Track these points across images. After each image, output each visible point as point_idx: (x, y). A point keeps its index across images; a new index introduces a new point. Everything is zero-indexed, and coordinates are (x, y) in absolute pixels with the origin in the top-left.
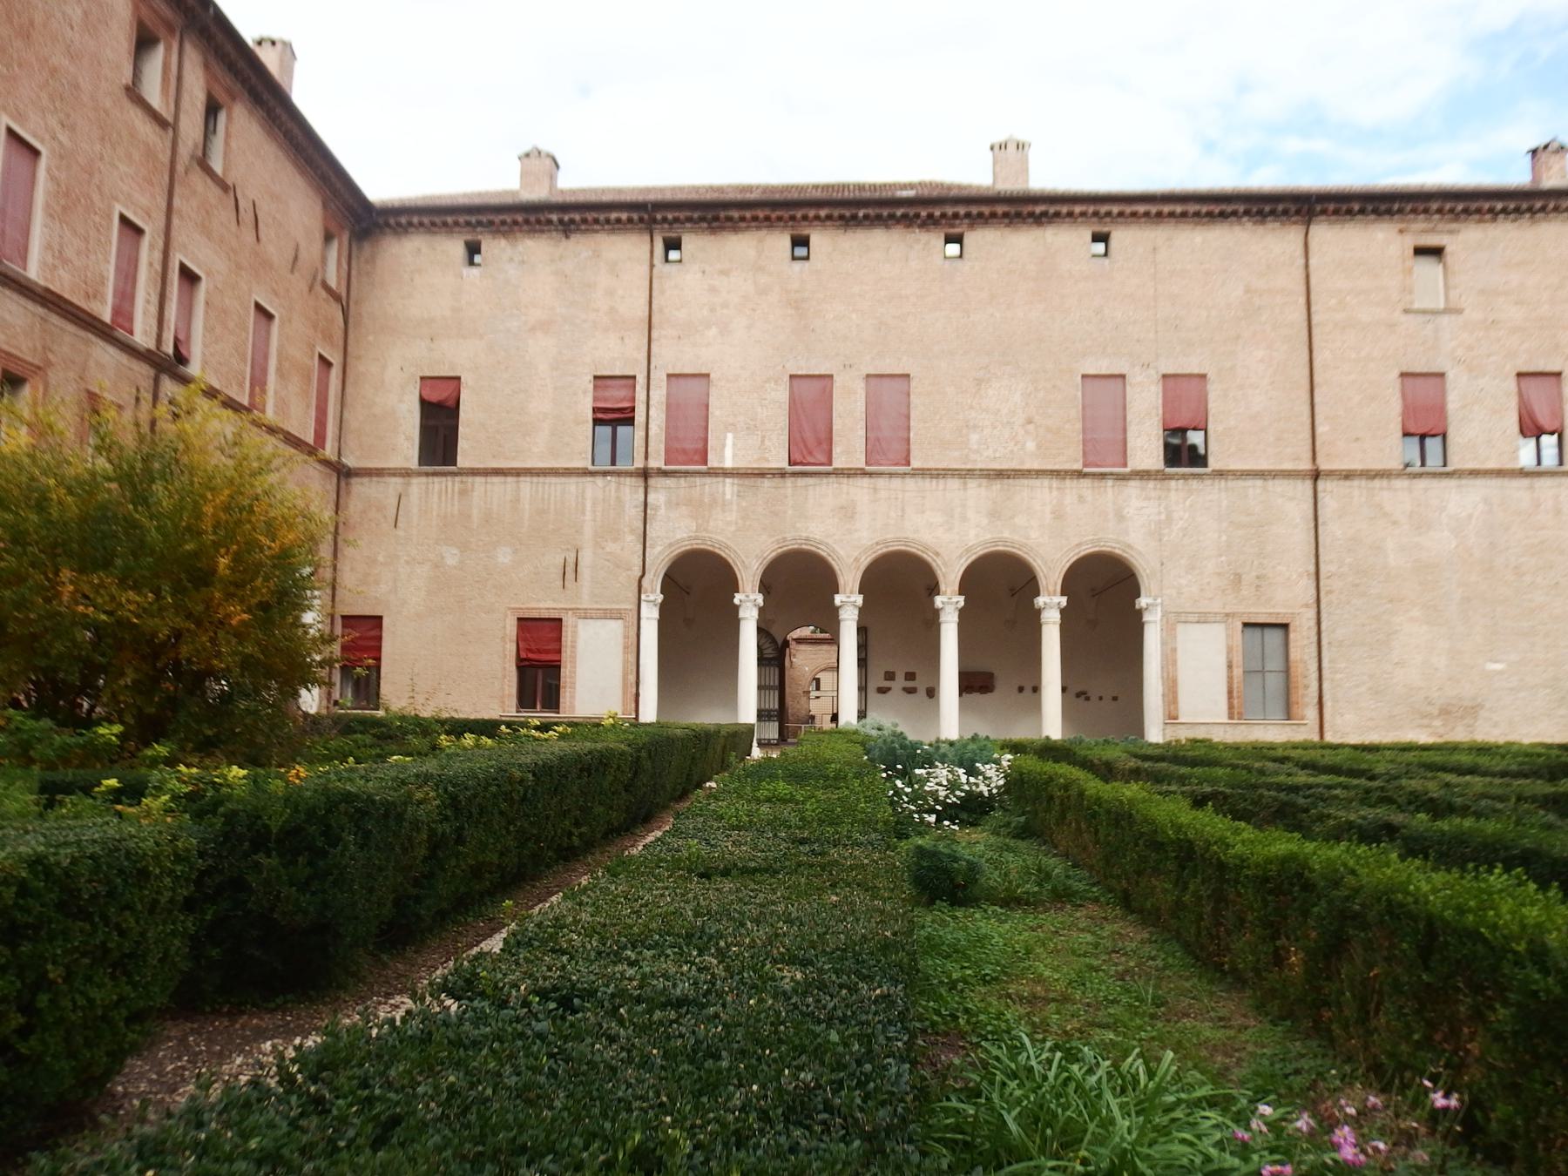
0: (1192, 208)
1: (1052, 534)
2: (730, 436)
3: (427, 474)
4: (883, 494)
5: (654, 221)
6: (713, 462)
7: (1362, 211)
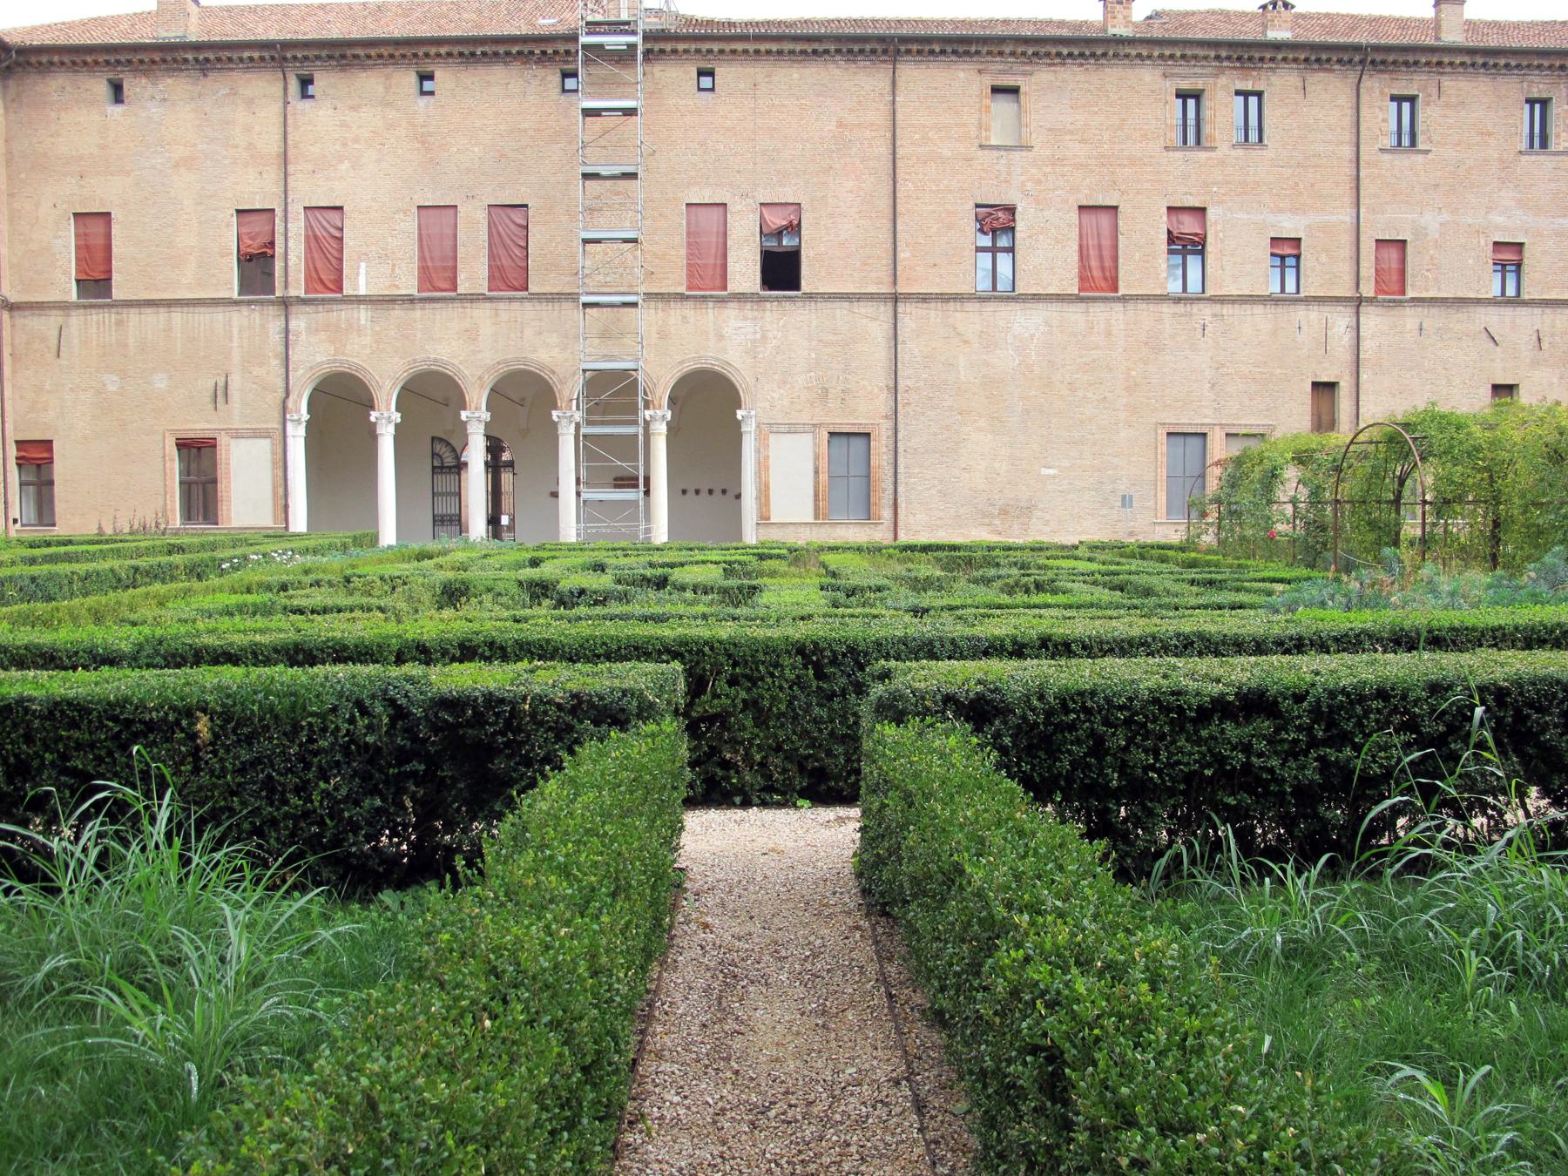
0: (787, 46)
2: (363, 265)
3: (85, 307)
4: (504, 316)
5: (285, 59)
6: (348, 290)
7: (943, 52)
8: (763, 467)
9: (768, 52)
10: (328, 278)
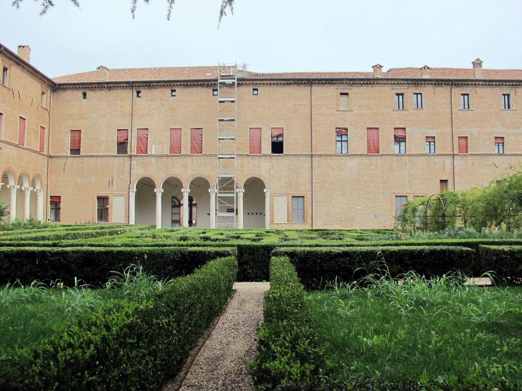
0: (279, 82)
1: (241, 172)
2: (154, 146)
3: (72, 157)
5: (133, 86)
7: (325, 83)
8: (272, 206)
9: (274, 84)
10: (143, 149)
